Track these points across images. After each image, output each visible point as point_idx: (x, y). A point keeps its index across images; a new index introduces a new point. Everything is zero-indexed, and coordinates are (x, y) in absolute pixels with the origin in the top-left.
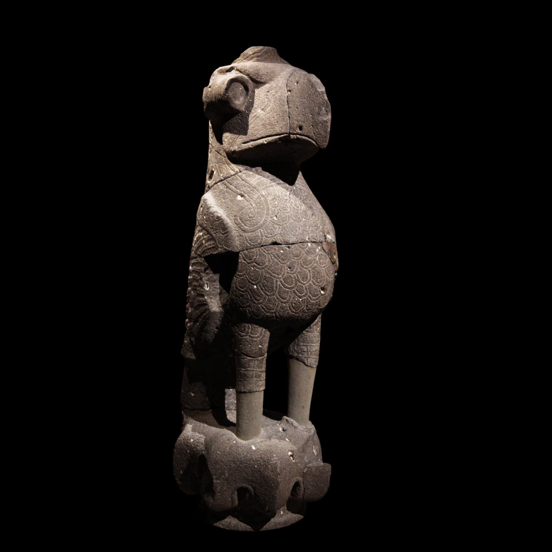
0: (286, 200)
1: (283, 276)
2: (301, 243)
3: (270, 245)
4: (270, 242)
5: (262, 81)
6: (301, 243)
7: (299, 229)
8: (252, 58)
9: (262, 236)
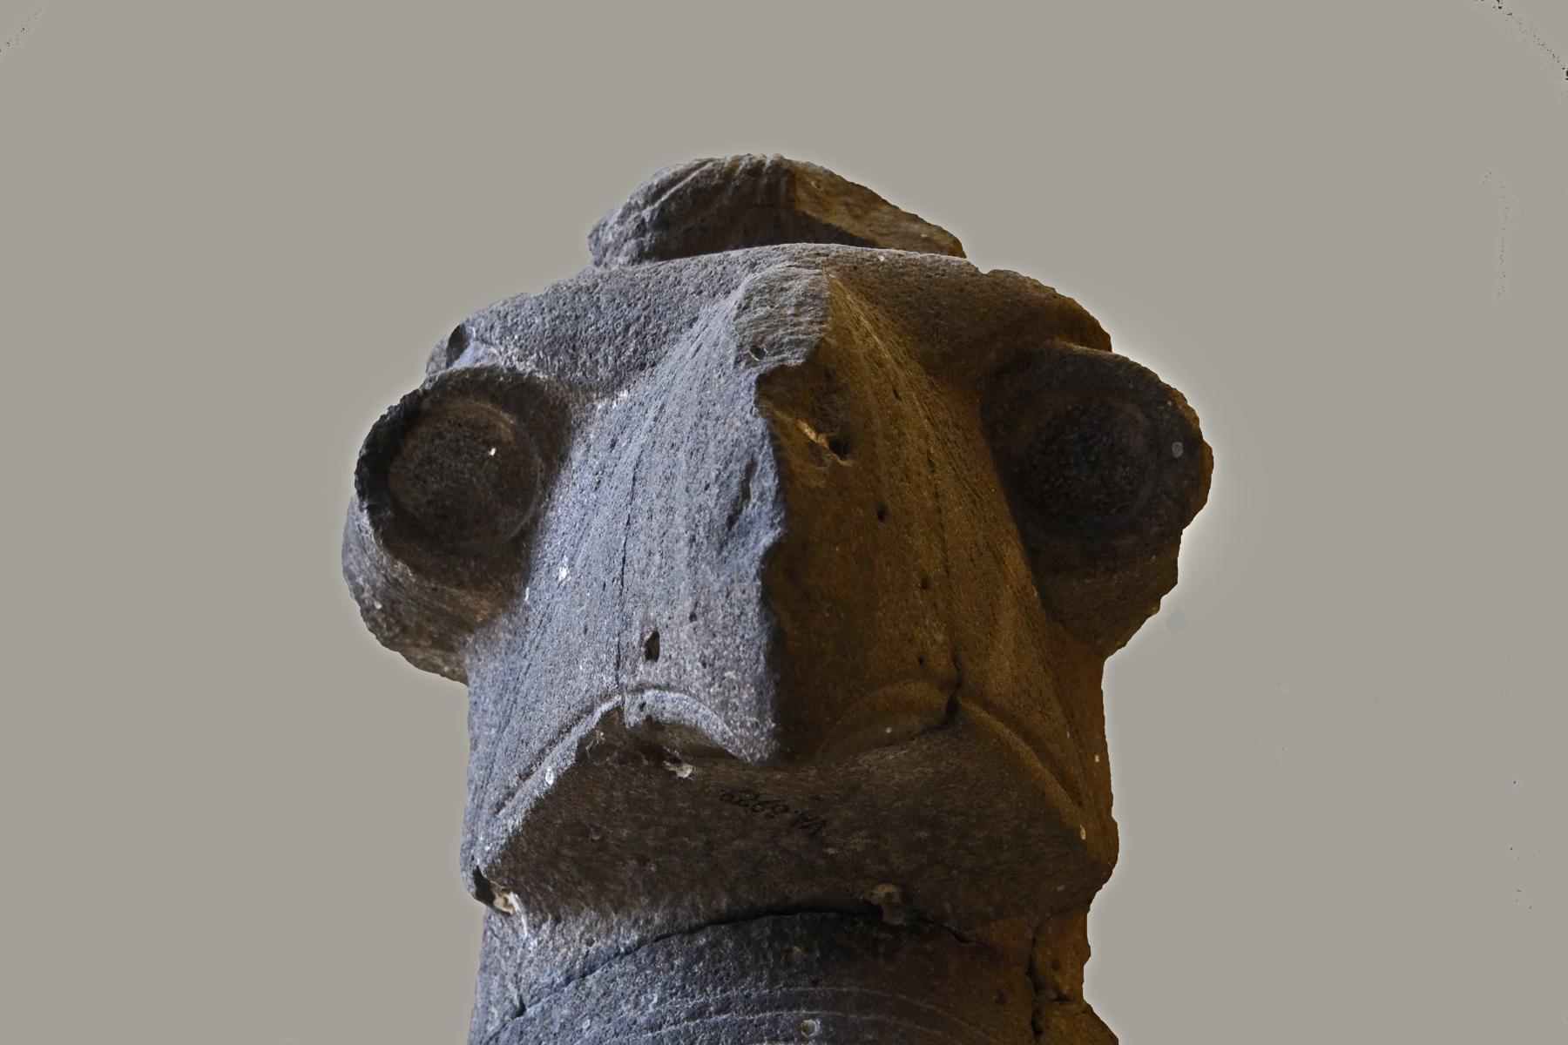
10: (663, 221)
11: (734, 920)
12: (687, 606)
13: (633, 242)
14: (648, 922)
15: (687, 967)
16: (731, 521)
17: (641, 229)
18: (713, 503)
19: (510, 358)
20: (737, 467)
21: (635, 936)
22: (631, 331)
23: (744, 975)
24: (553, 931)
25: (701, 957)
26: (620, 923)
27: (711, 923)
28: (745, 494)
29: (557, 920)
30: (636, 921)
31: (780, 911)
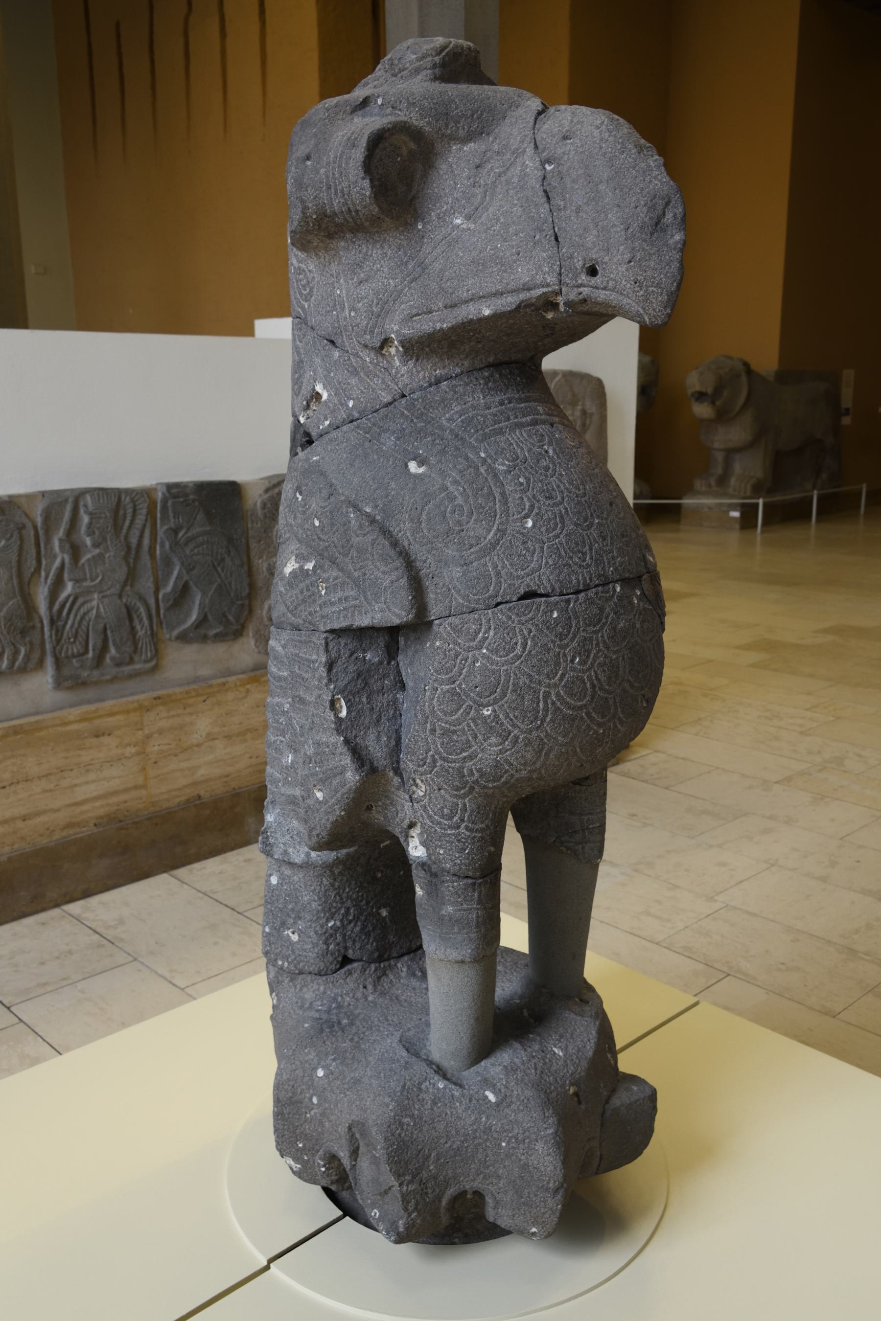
0: (547, 469)
1: (561, 679)
2: (596, 586)
3: (520, 599)
4: (522, 591)
6: (596, 586)
7: (591, 549)
8: (417, 71)
9: (498, 574)
10: (443, 65)
11: (496, 366)
12: (627, 256)
13: (429, 72)
14: (463, 365)
15: (486, 384)
16: (657, 224)
17: (434, 66)
18: (643, 214)
19: (411, 118)
20: (661, 203)
21: (458, 370)
22: (475, 116)
23: (508, 388)
25: (490, 381)
26: (449, 365)
28: (664, 214)
29: (417, 360)
31: (507, 363)
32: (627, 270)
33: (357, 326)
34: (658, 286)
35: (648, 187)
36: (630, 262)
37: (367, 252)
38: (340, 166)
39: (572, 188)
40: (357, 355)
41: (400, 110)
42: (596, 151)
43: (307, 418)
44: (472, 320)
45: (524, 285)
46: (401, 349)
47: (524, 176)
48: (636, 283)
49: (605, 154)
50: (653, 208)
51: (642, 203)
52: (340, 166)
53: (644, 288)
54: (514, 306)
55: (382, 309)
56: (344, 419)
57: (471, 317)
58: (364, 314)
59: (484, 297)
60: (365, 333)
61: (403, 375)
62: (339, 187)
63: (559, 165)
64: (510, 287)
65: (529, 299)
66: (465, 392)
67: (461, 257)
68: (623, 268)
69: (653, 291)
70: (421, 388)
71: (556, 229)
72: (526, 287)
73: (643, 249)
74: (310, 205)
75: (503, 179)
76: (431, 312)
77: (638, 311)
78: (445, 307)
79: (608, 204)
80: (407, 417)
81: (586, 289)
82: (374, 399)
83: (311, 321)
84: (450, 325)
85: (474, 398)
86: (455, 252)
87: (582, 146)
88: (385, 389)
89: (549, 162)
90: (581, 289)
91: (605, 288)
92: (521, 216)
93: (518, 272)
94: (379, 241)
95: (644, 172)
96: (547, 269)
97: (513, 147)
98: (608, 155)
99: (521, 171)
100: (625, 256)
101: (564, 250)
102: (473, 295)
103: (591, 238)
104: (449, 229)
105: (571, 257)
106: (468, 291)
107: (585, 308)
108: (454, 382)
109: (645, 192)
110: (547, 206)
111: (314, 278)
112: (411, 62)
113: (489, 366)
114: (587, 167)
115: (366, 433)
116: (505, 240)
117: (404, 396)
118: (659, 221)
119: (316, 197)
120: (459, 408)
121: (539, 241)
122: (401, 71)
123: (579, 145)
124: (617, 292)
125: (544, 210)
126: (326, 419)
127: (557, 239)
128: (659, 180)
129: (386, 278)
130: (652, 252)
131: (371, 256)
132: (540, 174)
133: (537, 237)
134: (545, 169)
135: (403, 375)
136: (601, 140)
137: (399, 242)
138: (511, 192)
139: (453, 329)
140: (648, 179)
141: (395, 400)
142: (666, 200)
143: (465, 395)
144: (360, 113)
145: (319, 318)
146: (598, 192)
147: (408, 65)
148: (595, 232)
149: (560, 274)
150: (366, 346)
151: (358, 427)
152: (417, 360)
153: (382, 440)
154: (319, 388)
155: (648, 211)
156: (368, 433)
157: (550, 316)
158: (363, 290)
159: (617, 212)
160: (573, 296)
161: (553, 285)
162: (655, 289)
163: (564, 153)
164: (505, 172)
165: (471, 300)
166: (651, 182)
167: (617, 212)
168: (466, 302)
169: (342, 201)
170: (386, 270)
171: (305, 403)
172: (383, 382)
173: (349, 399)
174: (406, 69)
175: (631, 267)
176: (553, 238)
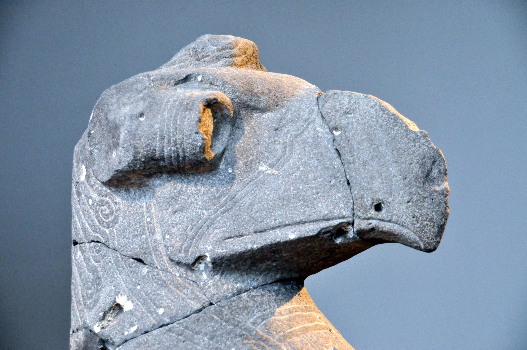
5: (261, 105)
8: (218, 58)
12: (407, 198)
14: (258, 280)
16: (427, 176)
18: (416, 169)
20: (429, 162)
21: (255, 284)
24: (220, 278)
27: (275, 282)
30: (254, 279)
32: (407, 208)
33: (172, 246)
34: (431, 220)
35: (418, 150)
36: (409, 202)
37: (182, 188)
38: (175, 123)
39: (358, 148)
40: (167, 271)
41: (217, 86)
42: (374, 123)
43: (103, 328)
44: (279, 242)
45: (324, 216)
46: (210, 265)
47: (316, 137)
48: (413, 217)
49: (381, 126)
50: (423, 165)
51: (415, 161)
52: (175, 123)
53: (420, 222)
54: (316, 232)
55: (198, 232)
56: (154, 325)
57: (278, 240)
58: (180, 237)
59: (289, 225)
60: (180, 252)
61: (209, 287)
62: (173, 139)
63: (345, 132)
64: (311, 218)
65: (328, 227)
66: (263, 301)
67: (268, 195)
68: (404, 207)
69: (427, 224)
70: (226, 298)
71: (348, 177)
72: (326, 218)
73: (419, 194)
74: (142, 151)
75: (299, 139)
76: (242, 236)
77: (415, 239)
78: (256, 232)
79: (389, 161)
80: (217, 321)
81: (374, 221)
82: (185, 306)
83: (113, 243)
84: (260, 246)
85: (270, 306)
86: (262, 190)
87: (362, 119)
88: (194, 298)
89: (336, 129)
90: (371, 221)
91: (390, 221)
92: (318, 166)
93: (318, 207)
94: (192, 181)
95: (414, 140)
96: (343, 206)
97: (304, 118)
98: (384, 127)
99: (314, 134)
100: (405, 198)
101: (356, 192)
102: (280, 223)
103: (376, 185)
104: (256, 174)
105: (362, 197)
106: (275, 220)
107: (372, 235)
108: (253, 293)
109: (417, 153)
110: (339, 160)
111: (119, 209)
112: (213, 52)
113: (277, 281)
114: (368, 134)
115: (179, 335)
116: (306, 183)
117: (211, 304)
118: (429, 174)
119: (148, 145)
120: (260, 314)
121: (335, 185)
122: (203, 57)
123: (360, 118)
124: (399, 224)
125: (337, 162)
126: (132, 325)
127: (349, 183)
128: (427, 146)
129: (199, 209)
130: (425, 196)
131: (186, 191)
132: (330, 137)
133: (333, 182)
134: (333, 134)
135: (209, 287)
136: (377, 116)
137: (212, 182)
138: (307, 149)
139: (261, 249)
140: (417, 145)
141: (204, 308)
142: (433, 160)
143: (262, 304)
144: (182, 85)
145: (124, 241)
146: (379, 152)
147: (210, 53)
148: (380, 180)
149: (353, 209)
150: (178, 263)
151: (170, 330)
152: (222, 274)
153: (196, 341)
154: (121, 300)
155: (420, 167)
156: (181, 335)
157: (339, 241)
158: (177, 218)
159: (396, 167)
160: (364, 225)
161: (348, 217)
162: (429, 223)
163: (348, 124)
164: (300, 135)
165: (279, 227)
166: (420, 147)
167: (396, 167)
168: (274, 228)
169: (173, 149)
170: (200, 203)
171: (101, 314)
172: (193, 293)
173: (158, 307)
174: (208, 56)
175: (409, 206)
176: (346, 183)
